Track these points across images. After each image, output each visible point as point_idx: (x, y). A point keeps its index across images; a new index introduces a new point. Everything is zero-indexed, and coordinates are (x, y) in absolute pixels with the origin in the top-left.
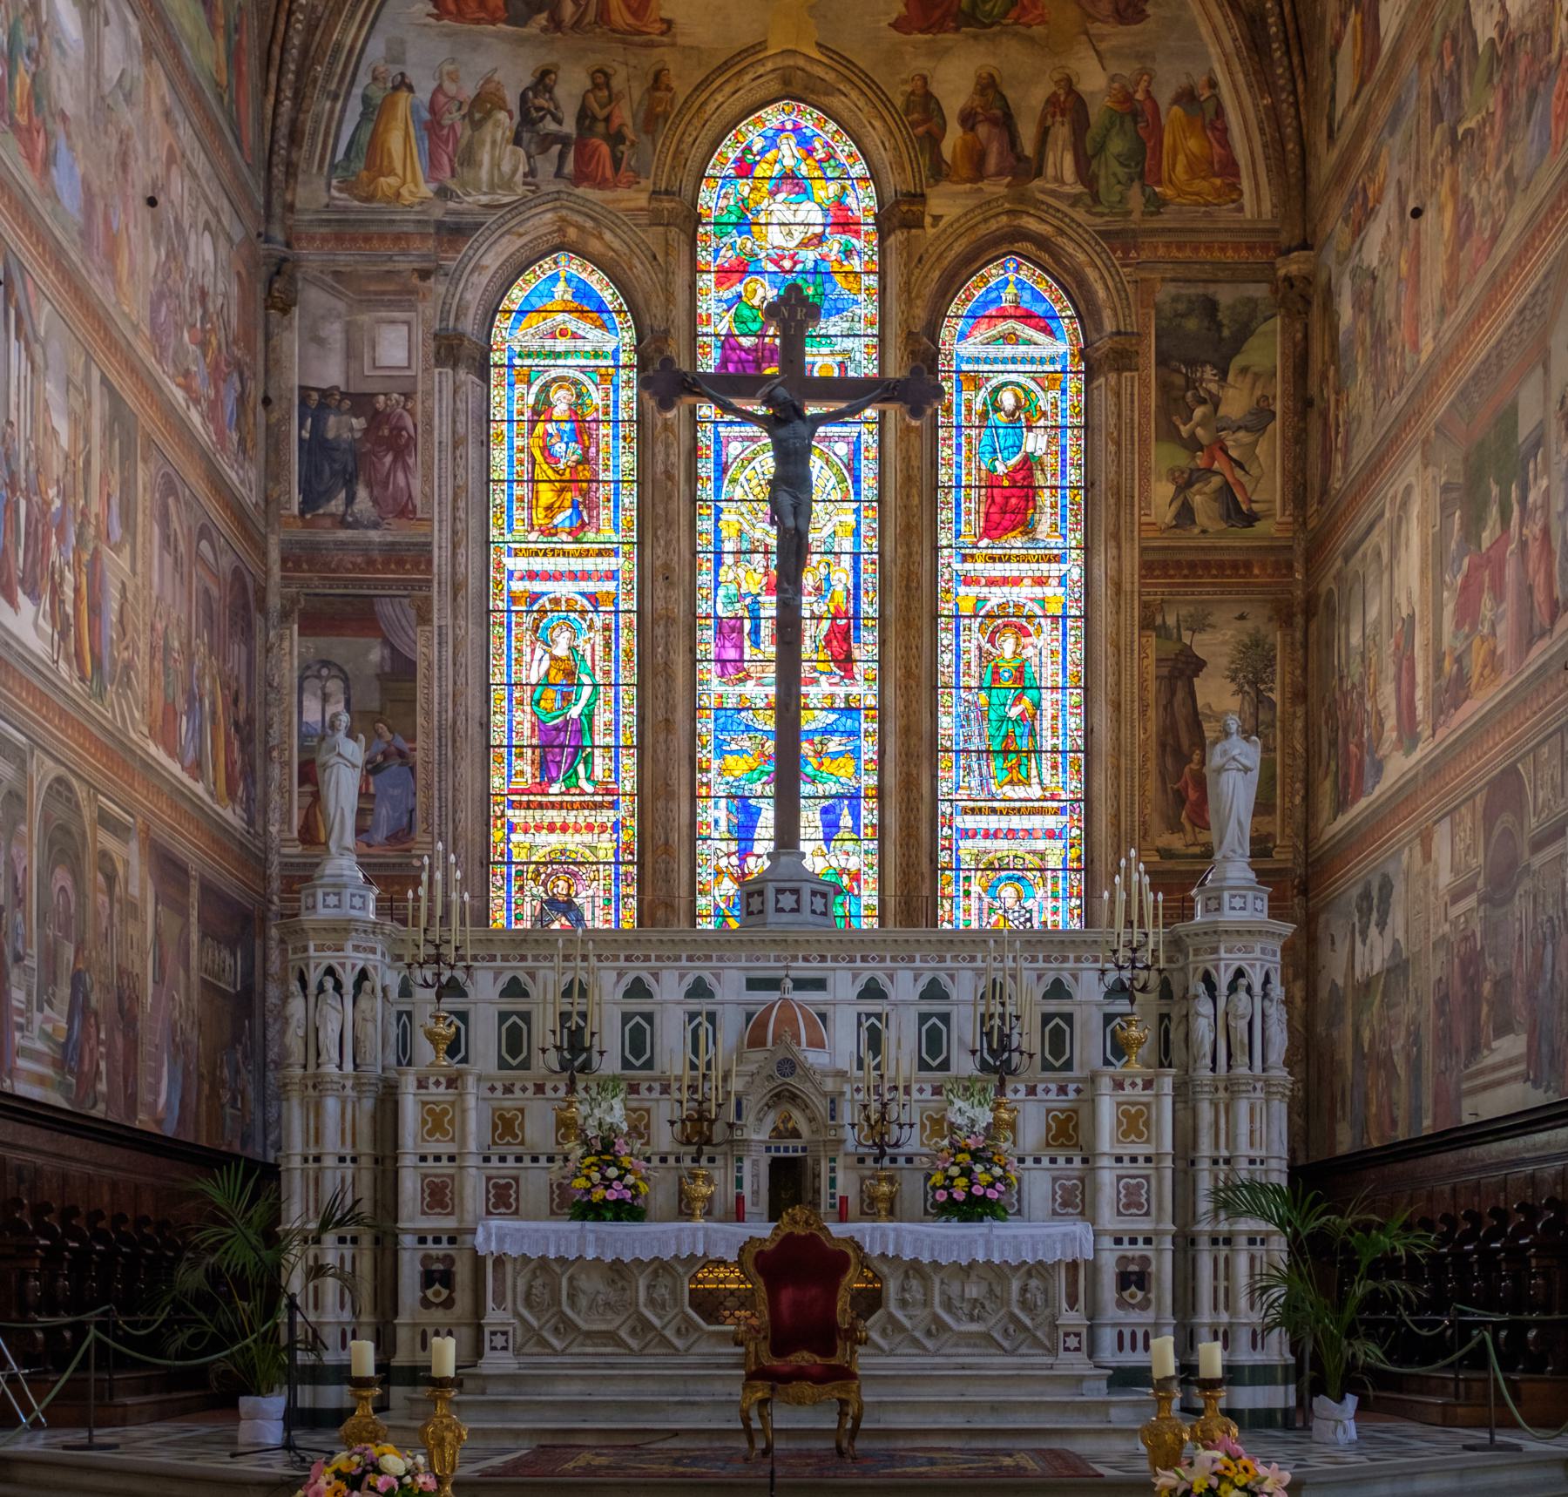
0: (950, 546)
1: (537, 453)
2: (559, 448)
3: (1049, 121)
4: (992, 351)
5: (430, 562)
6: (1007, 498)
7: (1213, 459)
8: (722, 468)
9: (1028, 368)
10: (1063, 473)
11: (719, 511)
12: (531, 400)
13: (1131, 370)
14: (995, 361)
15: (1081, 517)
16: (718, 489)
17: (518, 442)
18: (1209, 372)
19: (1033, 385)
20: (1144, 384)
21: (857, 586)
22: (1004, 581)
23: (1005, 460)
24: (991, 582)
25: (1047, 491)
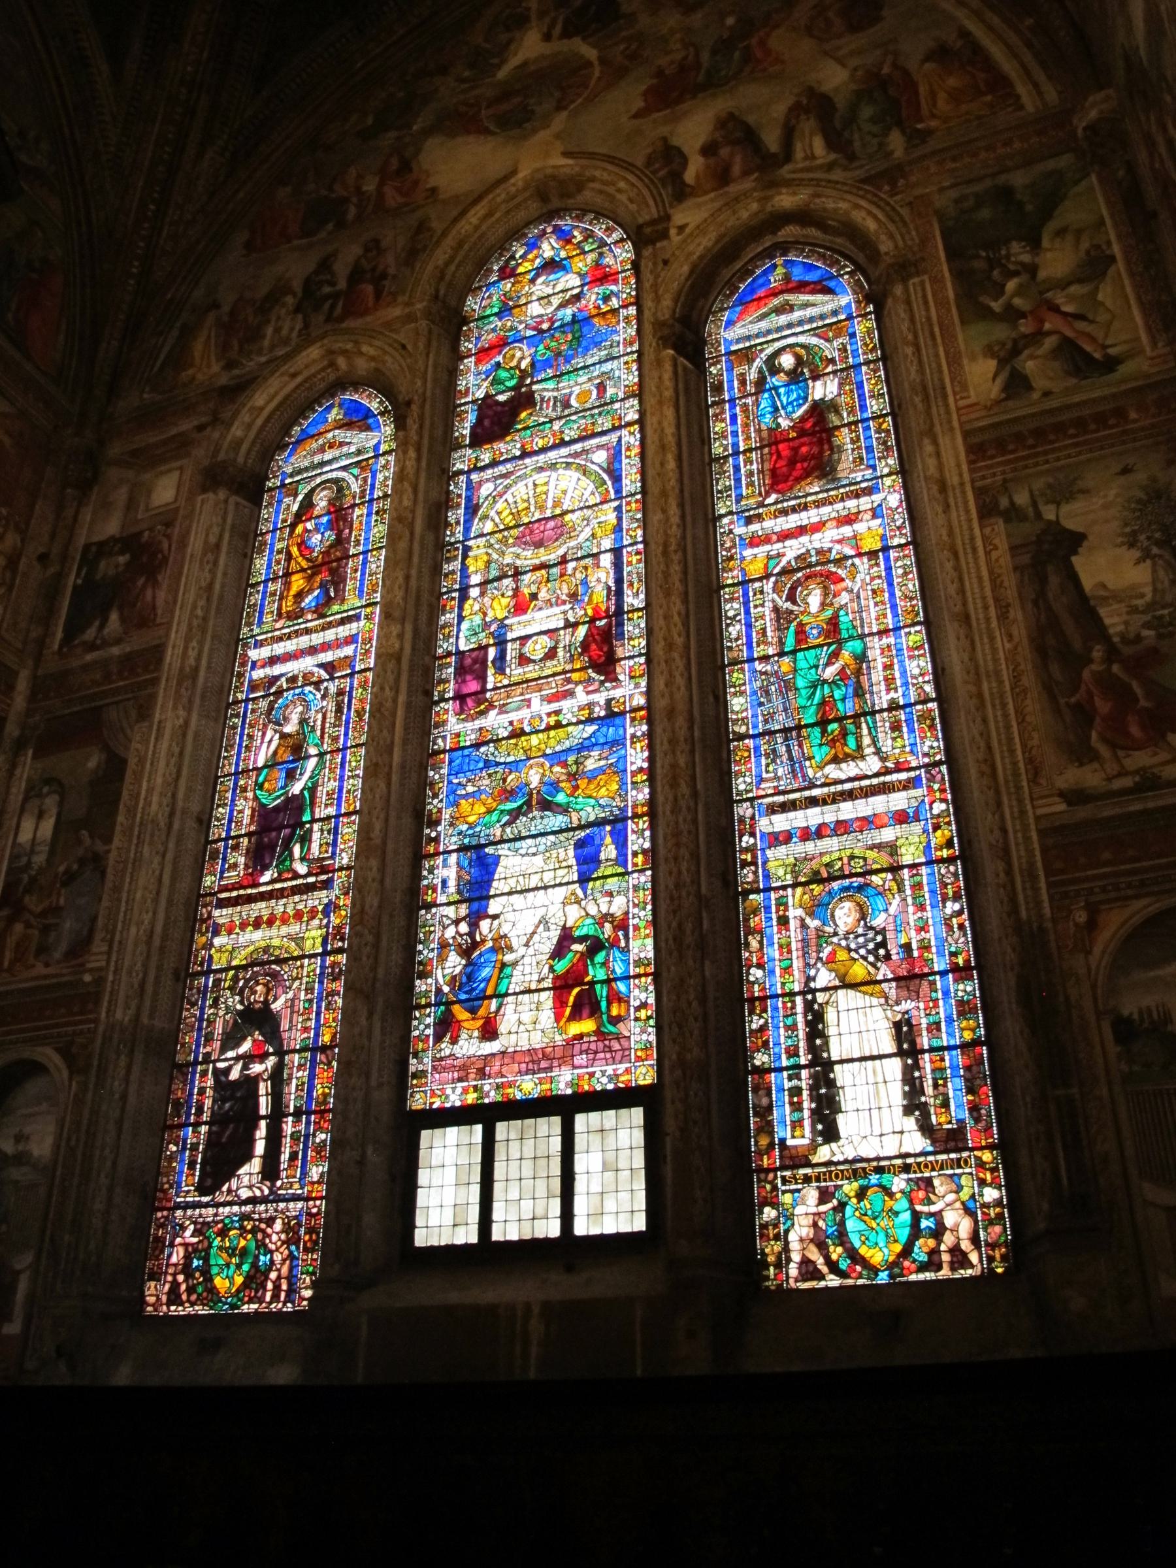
0: (731, 513)
1: (295, 551)
2: (316, 539)
3: (793, 121)
4: (764, 325)
5: (160, 661)
6: (795, 450)
7: (1042, 322)
8: (472, 509)
9: (807, 327)
10: (863, 408)
11: (467, 549)
12: (295, 508)
13: (918, 274)
14: (769, 332)
15: (892, 442)
16: (467, 530)
17: (279, 546)
18: (1015, 247)
19: (814, 341)
20: (937, 280)
21: (619, 581)
22: (801, 531)
23: (788, 415)
24: (785, 536)
25: (845, 430)
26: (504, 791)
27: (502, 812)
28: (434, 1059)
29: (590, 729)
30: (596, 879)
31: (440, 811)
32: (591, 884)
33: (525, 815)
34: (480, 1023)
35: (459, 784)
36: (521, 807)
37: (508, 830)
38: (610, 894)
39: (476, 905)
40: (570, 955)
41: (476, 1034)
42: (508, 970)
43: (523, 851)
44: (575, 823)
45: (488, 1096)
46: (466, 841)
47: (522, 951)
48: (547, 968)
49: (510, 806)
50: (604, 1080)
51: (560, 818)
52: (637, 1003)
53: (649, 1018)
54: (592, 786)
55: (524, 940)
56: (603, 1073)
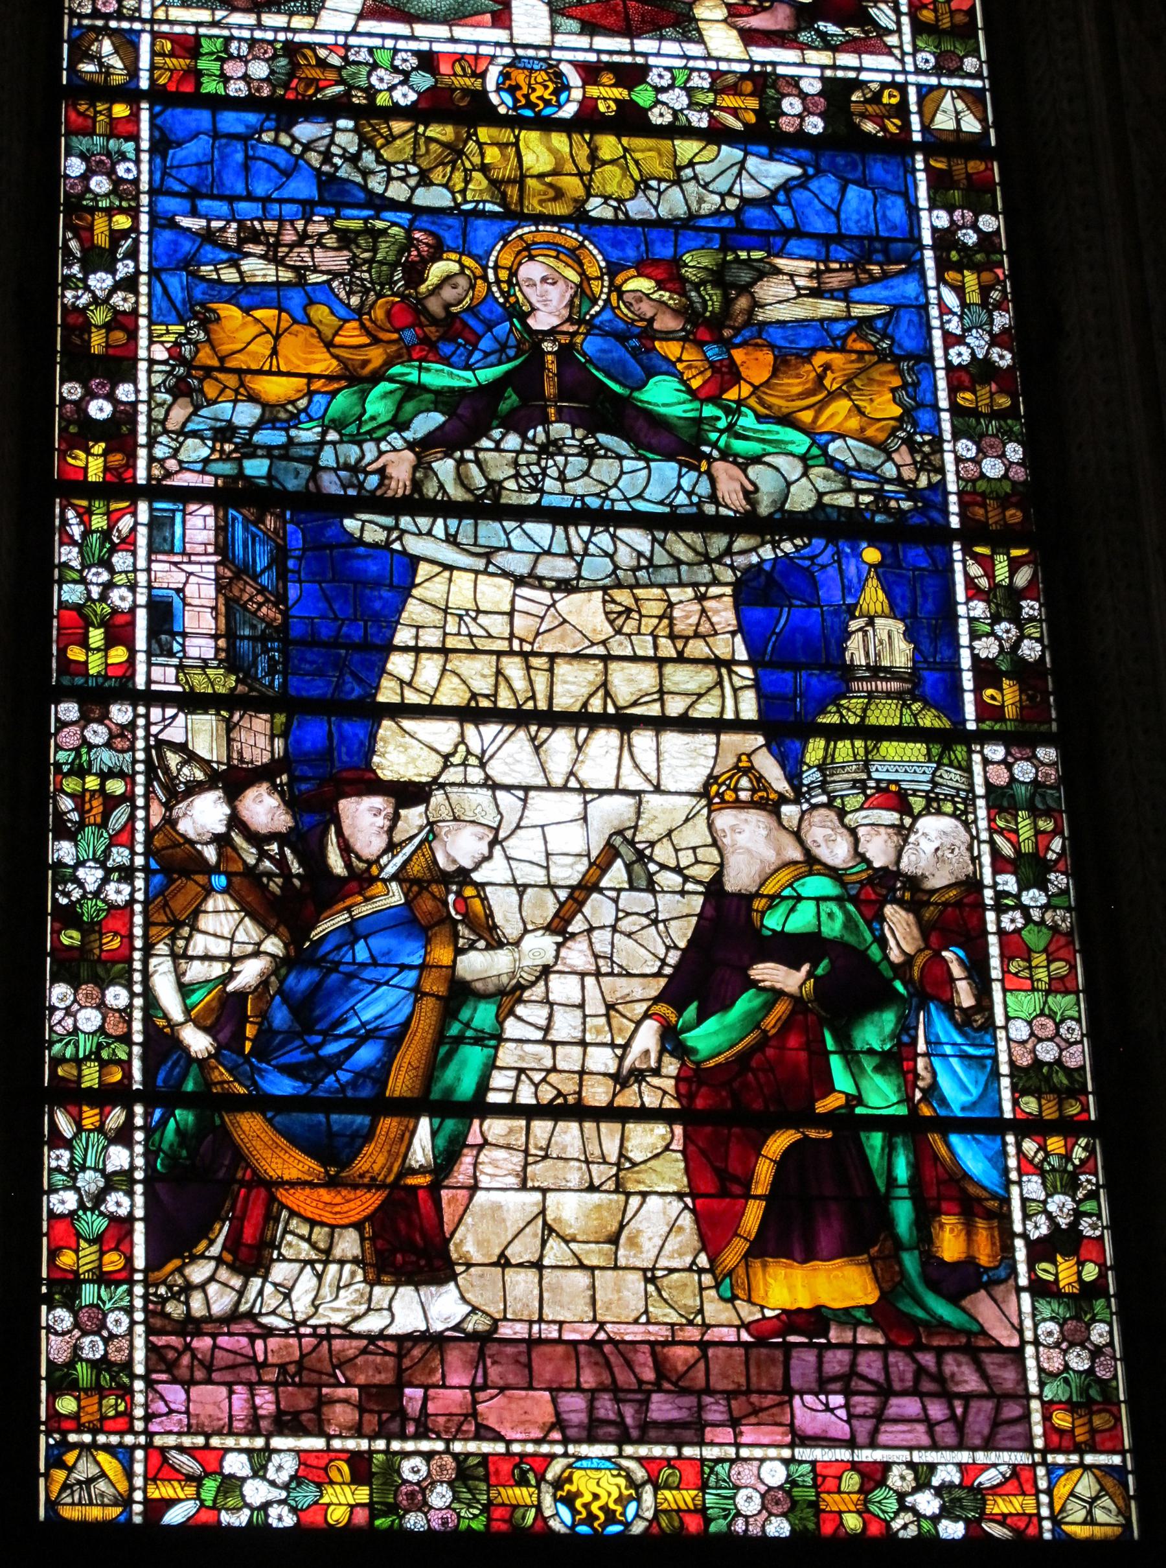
26: (417, 309)
27: (412, 391)
28: (157, 1321)
29: (778, 171)
30: (835, 733)
31: (124, 322)
32: (815, 750)
33: (517, 423)
34: (367, 1202)
35: (208, 236)
36: (495, 389)
37: (445, 468)
38: (898, 800)
39: (314, 732)
40: (745, 1003)
41: (348, 1244)
42: (483, 1015)
43: (519, 564)
44: (733, 499)
45: (424, 1507)
46: (256, 467)
47: (540, 947)
48: (650, 1028)
49: (438, 377)
50: (927, 1503)
51: (667, 470)
52: (1040, 1229)
53: (1090, 1291)
54: (793, 384)
55: (547, 907)
56: (923, 1475)
